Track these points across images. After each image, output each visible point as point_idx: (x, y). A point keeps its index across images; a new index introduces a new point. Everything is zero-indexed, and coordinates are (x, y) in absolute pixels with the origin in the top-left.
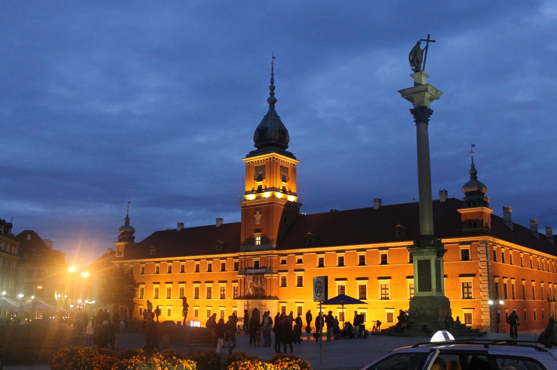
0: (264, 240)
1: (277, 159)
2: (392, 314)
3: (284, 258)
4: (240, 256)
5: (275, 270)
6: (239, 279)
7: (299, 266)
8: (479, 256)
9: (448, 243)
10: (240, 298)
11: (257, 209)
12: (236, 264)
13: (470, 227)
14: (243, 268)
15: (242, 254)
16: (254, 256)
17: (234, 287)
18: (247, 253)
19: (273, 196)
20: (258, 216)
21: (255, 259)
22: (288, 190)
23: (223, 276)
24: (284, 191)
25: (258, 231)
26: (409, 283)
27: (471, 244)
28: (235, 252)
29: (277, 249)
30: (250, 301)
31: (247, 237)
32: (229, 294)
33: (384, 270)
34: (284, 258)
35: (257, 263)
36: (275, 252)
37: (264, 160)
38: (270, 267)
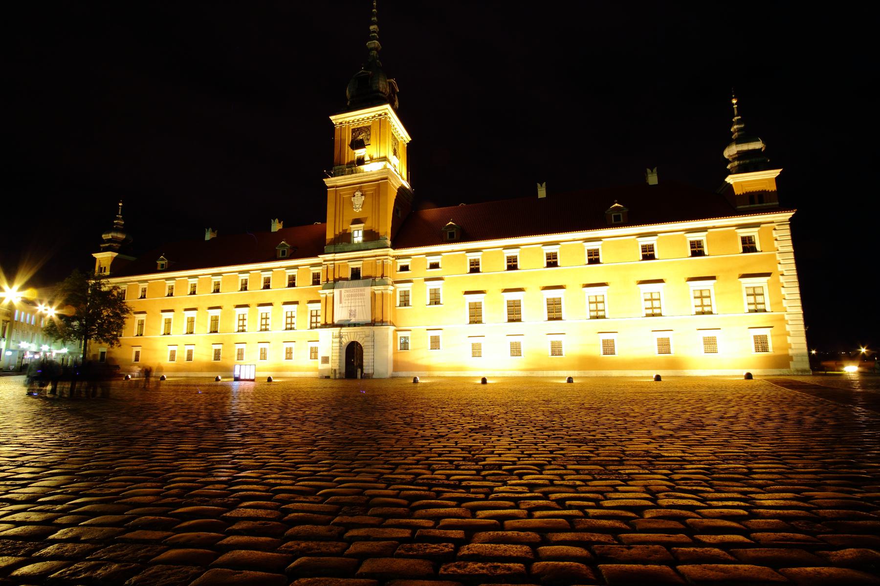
0: (372, 237)
5: (390, 281)
9: (714, 227)
13: (752, 202)
19: (385, 168)
20: (358, 200)
23: (290, 294)
25: (357, 221)
28: (315, 255)
29: (395, 246)
31: (337, 233)
32: (302, 322)
36: (391, 252)
38: (382, 276)
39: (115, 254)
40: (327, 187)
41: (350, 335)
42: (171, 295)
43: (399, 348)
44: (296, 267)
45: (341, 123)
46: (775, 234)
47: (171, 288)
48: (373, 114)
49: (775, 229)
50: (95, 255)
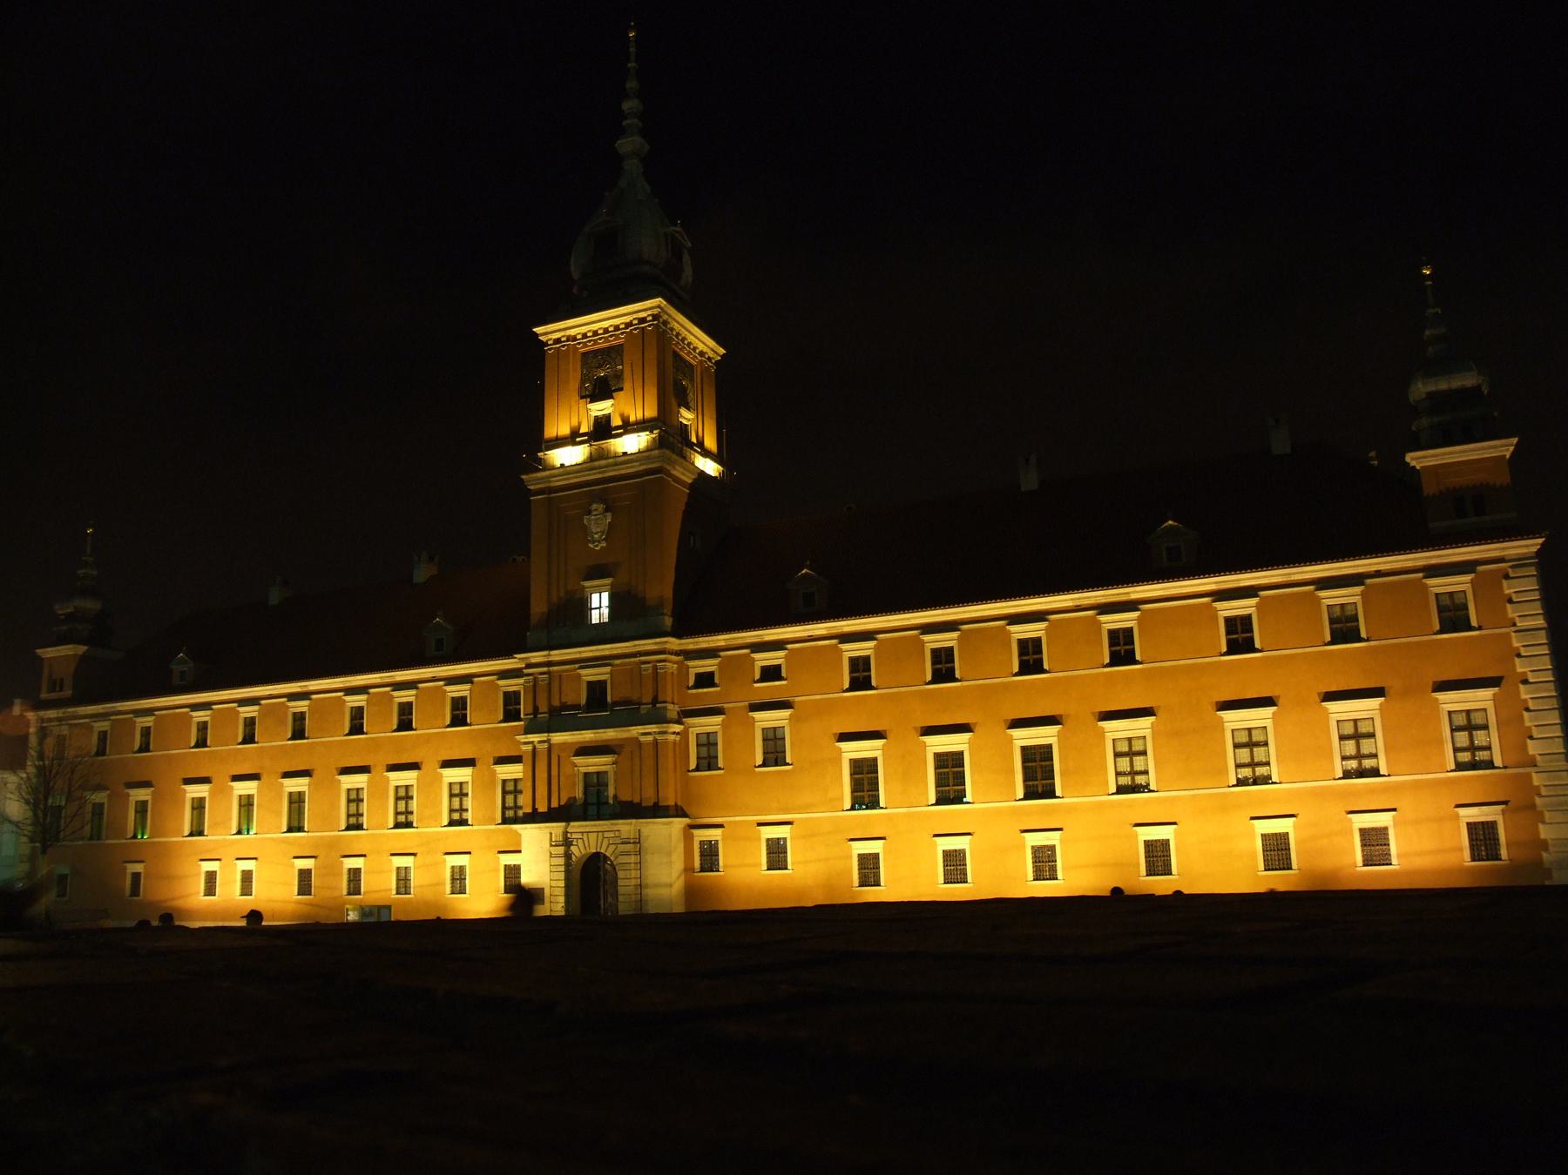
2: (876, 856)
3: (708, 665)
4: (529, 666)
5: (672, 710)
6: (530, 747)
8: (1511, 611)
9: (1378, 574)
10: (533, 817)
12: (511, 699)
14: (543, 707)
15: (537, 657)
17: (504, 781)
18: (557, 655)
20: (598, 523)
21: (590, 675)
22: (694, 440)
23: (459, 741)
25: (597, 572)
27: (1473, 571)
28: (507, 653)
30: (576, 826)
31: (555, 599)
33: (1127, 685)
34: (708, 665)
35: (597, 689)
36: (673, 643)
37: (617, 328)
38: (655, 701)
42: (202, 743)
46: (1508, 589)
47: (203, 727)
48: (627, 319)
49: (1507, 577)
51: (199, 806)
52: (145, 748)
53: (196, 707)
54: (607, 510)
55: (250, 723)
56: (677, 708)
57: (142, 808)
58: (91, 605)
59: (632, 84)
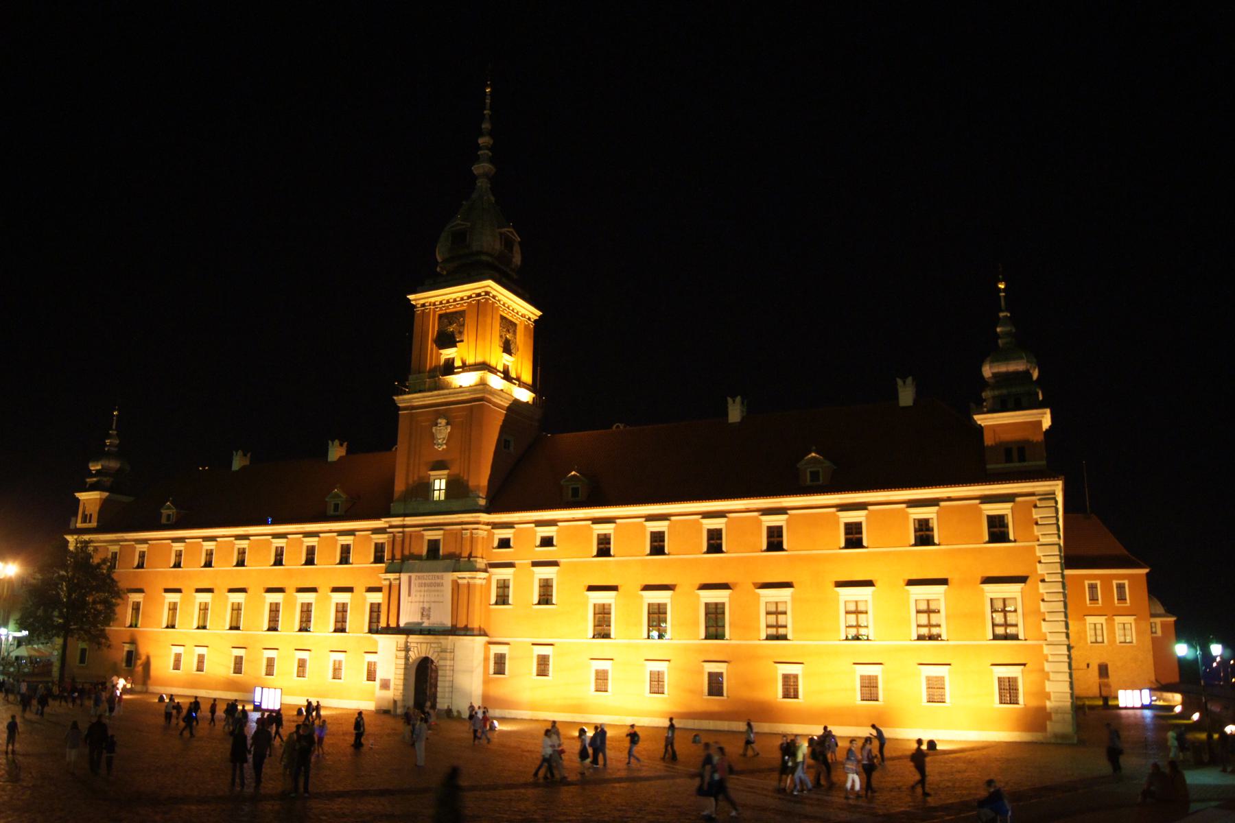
0: (457, 489)
1: (494, 297)
4: (391, 527)
5: (481, 563)
6: (387, 583)
7: (504, 555)
8: (1037, 531)
9: (949, 499)
11: (439, 415)
12: (379, 549)
13: (1009, 459)
14: (398, 556)
15: (396, 521)
16: (423, 528)
18: (409, 520)
19: (483, 383)
20: (442, 431)
21: (430, 535)
22: (513, 375)
24: (506, 376)
25: (439, 465)
26: (842, 599)
27: (1013, 501)
29: (488, 510)
30: (413, 638)
31: (411, 482)
32: (358, 620)
33: (775, 566)
35: (434, 546)
36: (484, 517)
37: (462, 299)
38: (470, 556)
39: (106, 494)
40: (398, 409)
41: (420, 647)
42: (177, 565)
43: (492, 670)
44: (351, 533)
45: (423, 305)
46: (1036, 514)
47: (179, 554)
48: (468, 293)
49: (1035, 506)
50: (77, 495)
51: (173, 608)
52: (141, 566)
53: (175, 540)
54: (448, 424)
55: (210, 554)
56: (485, 561)
57: (136, 608)
58: (114, 464)
59: (486, 126)
